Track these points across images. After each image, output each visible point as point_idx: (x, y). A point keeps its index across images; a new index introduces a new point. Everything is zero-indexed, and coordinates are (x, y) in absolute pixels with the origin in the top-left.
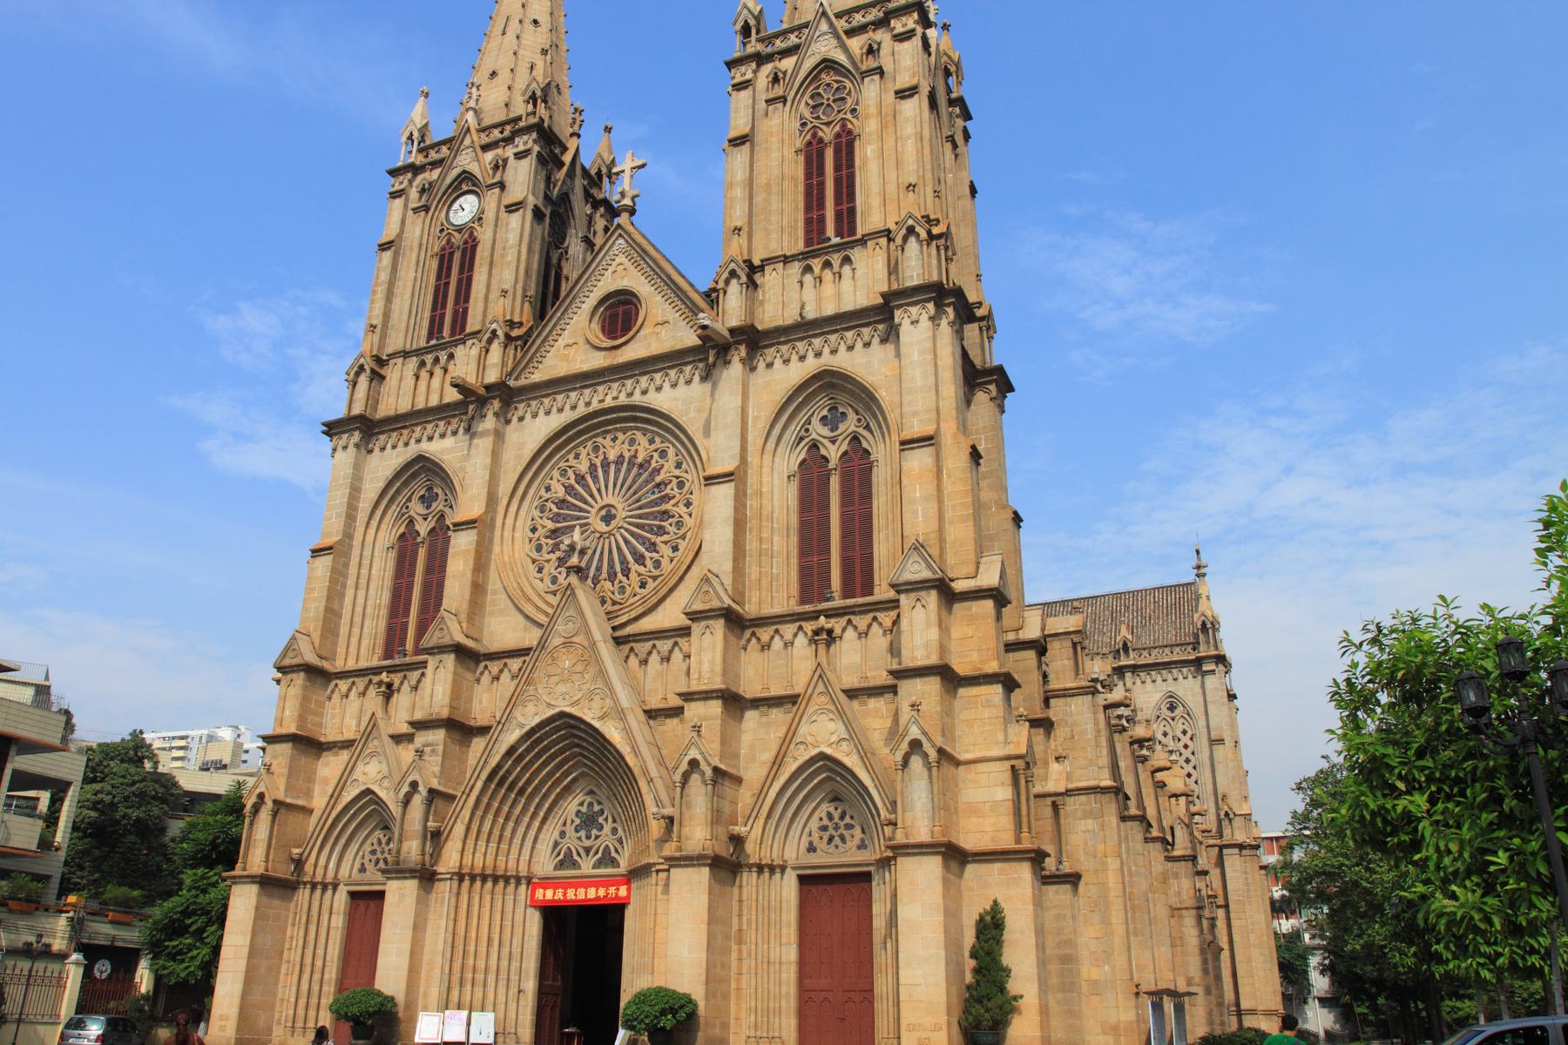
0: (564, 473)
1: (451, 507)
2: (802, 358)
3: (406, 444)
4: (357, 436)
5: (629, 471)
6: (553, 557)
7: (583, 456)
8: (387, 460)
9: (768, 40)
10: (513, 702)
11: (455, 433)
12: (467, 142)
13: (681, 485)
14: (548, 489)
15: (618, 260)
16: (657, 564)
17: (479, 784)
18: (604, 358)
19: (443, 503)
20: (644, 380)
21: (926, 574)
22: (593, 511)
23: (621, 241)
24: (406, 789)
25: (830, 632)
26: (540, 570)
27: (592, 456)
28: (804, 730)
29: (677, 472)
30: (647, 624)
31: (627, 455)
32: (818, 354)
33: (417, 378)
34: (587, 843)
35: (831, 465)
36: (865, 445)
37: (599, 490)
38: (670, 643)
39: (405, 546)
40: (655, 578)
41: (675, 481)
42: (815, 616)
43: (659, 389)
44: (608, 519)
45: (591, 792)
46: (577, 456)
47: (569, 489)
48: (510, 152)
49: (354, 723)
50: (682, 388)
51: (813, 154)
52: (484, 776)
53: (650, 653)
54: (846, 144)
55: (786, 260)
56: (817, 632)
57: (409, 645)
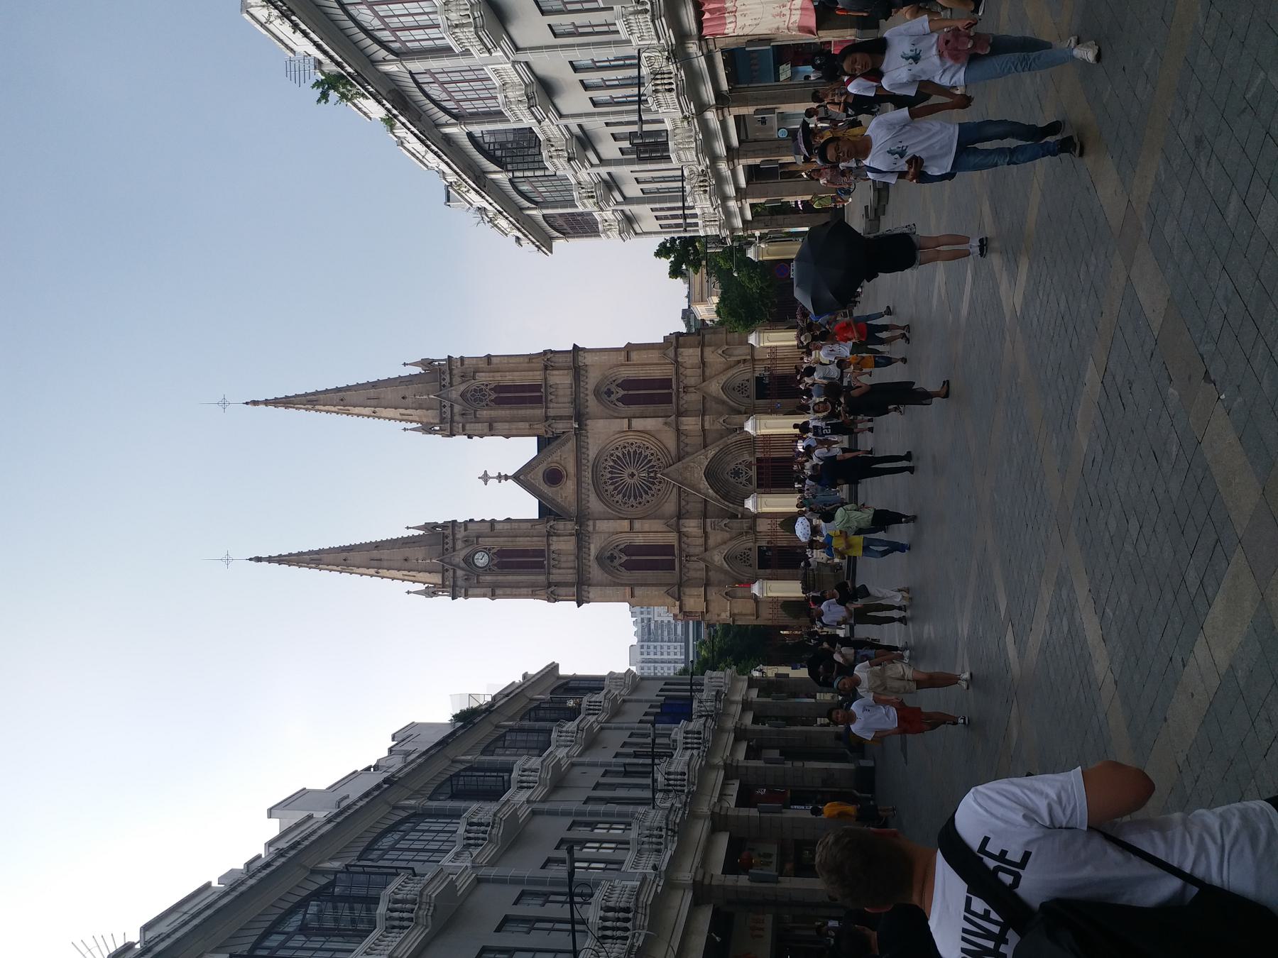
0: (613, 496)
1: (617, 546)
2: (587, 401)
3: (590, 566)
4: (583, 587)
5: (616, 468)
6: (644, 496)
7: (607, 488)
8: (595, 572)
9: (442, 420)
10: (700, 493)
11: (589, 544)
12: (447, 560)
13: (625, 447)
14: (617, 502)
15: (529, 478)
16: (652, 454)
17: (726, 503)
18: (570, 480)
19: (616, 550)
20: (584, 462)
21: (673, 351)
22: (629, 480)
23: (521, 477)
24: (727, 528)
25: (684, 388)
26: (648, 502)
27: (608, 484)
28: (714, 395)
29: (620, 449)
30: (673, 455)
31: (610, 469)
32: (587, 395)
33: (559, 568)
34: (744, 473)
35: (626, 392)
36: (620, 381)
37: (621, 480)
38: (681, 443)
39: (630, 566)
40: (657, 455)
41: (623, 450)
42: (678, 391)
43: (588, 455)
44: (632, 475)
45: (727, 474)
46: (606, 491)
47: (619, 493)
48: (461, 534)
49: (699, 573)
50: (590, 447)
51: (499, 402)
52: (723, 501)
53: (684, 451)
54: (499, 389)
55: (547, 408)
56: (684, 392)
57: (670, 558)
